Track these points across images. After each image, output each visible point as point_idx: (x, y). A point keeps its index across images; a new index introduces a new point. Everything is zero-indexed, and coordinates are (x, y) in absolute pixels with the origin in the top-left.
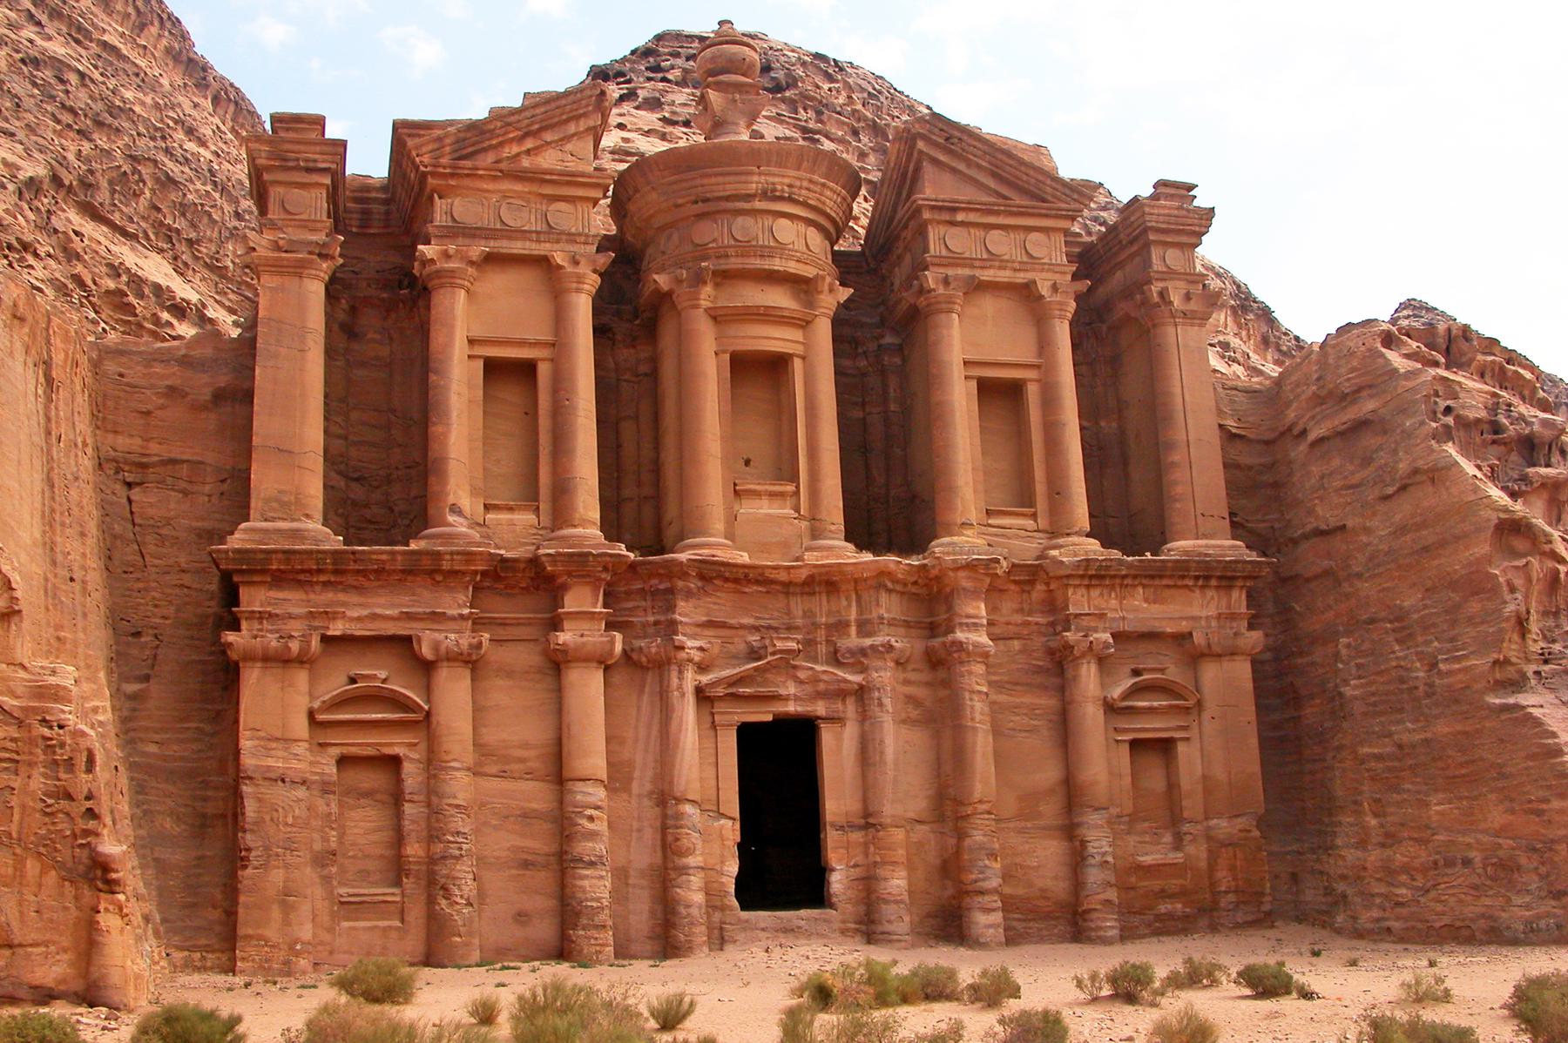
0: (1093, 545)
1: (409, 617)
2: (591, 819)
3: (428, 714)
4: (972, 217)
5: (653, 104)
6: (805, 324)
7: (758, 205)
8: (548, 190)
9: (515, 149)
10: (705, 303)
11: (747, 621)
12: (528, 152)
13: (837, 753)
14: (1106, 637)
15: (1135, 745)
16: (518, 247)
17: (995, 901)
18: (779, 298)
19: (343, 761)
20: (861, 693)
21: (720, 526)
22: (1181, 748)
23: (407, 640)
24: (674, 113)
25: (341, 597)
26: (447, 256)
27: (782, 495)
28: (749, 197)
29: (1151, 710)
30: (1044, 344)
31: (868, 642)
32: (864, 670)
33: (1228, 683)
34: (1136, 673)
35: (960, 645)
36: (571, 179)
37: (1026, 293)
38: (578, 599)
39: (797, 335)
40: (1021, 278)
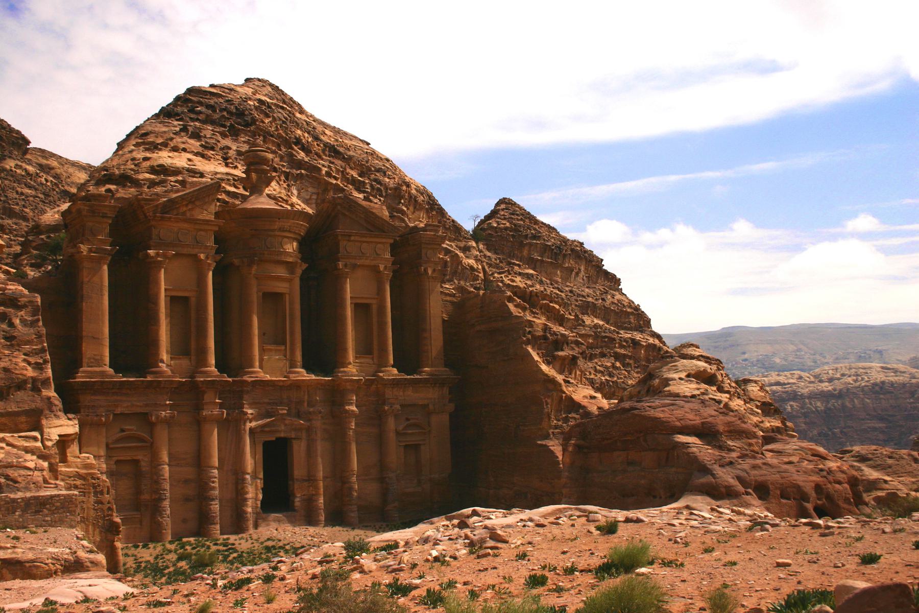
0: (395, 371)
1: (147, 405)
2: (213, 482)
3: (152, 443)
4: (357, 238)
5: (196, 136)
6: (290, 281)
7: (277, 233)
8: (197, 227)
9: (185, 209)
10: (253, 272)
11: (266, 400)
12: (189, 210)
13: (299, 450)
14: (398, 407)
15: (406, 446)
16: (185, 251)
17: (355, 508)
18: (281, 272)
19: (118, 462)
20: (309, 430)
21: (257, 364)
22: (422, 447)
23: (147, 414)
24: (206, 142)
25: (119, 398)
26: (158, 255)
27: (280, 350)
28: (274, 230)
29: (412, 434)
30: (380, 291)
31: (311, 410)
32: (310, 420)
33: (440, 421)
34: (407, 419)
35: (347, 411)
36: (207, 222)
37: (375, 269)
38: (208, 397)
39: (286, 285)
40: (373, 263)
